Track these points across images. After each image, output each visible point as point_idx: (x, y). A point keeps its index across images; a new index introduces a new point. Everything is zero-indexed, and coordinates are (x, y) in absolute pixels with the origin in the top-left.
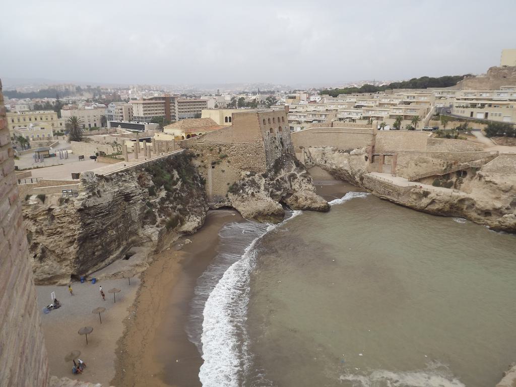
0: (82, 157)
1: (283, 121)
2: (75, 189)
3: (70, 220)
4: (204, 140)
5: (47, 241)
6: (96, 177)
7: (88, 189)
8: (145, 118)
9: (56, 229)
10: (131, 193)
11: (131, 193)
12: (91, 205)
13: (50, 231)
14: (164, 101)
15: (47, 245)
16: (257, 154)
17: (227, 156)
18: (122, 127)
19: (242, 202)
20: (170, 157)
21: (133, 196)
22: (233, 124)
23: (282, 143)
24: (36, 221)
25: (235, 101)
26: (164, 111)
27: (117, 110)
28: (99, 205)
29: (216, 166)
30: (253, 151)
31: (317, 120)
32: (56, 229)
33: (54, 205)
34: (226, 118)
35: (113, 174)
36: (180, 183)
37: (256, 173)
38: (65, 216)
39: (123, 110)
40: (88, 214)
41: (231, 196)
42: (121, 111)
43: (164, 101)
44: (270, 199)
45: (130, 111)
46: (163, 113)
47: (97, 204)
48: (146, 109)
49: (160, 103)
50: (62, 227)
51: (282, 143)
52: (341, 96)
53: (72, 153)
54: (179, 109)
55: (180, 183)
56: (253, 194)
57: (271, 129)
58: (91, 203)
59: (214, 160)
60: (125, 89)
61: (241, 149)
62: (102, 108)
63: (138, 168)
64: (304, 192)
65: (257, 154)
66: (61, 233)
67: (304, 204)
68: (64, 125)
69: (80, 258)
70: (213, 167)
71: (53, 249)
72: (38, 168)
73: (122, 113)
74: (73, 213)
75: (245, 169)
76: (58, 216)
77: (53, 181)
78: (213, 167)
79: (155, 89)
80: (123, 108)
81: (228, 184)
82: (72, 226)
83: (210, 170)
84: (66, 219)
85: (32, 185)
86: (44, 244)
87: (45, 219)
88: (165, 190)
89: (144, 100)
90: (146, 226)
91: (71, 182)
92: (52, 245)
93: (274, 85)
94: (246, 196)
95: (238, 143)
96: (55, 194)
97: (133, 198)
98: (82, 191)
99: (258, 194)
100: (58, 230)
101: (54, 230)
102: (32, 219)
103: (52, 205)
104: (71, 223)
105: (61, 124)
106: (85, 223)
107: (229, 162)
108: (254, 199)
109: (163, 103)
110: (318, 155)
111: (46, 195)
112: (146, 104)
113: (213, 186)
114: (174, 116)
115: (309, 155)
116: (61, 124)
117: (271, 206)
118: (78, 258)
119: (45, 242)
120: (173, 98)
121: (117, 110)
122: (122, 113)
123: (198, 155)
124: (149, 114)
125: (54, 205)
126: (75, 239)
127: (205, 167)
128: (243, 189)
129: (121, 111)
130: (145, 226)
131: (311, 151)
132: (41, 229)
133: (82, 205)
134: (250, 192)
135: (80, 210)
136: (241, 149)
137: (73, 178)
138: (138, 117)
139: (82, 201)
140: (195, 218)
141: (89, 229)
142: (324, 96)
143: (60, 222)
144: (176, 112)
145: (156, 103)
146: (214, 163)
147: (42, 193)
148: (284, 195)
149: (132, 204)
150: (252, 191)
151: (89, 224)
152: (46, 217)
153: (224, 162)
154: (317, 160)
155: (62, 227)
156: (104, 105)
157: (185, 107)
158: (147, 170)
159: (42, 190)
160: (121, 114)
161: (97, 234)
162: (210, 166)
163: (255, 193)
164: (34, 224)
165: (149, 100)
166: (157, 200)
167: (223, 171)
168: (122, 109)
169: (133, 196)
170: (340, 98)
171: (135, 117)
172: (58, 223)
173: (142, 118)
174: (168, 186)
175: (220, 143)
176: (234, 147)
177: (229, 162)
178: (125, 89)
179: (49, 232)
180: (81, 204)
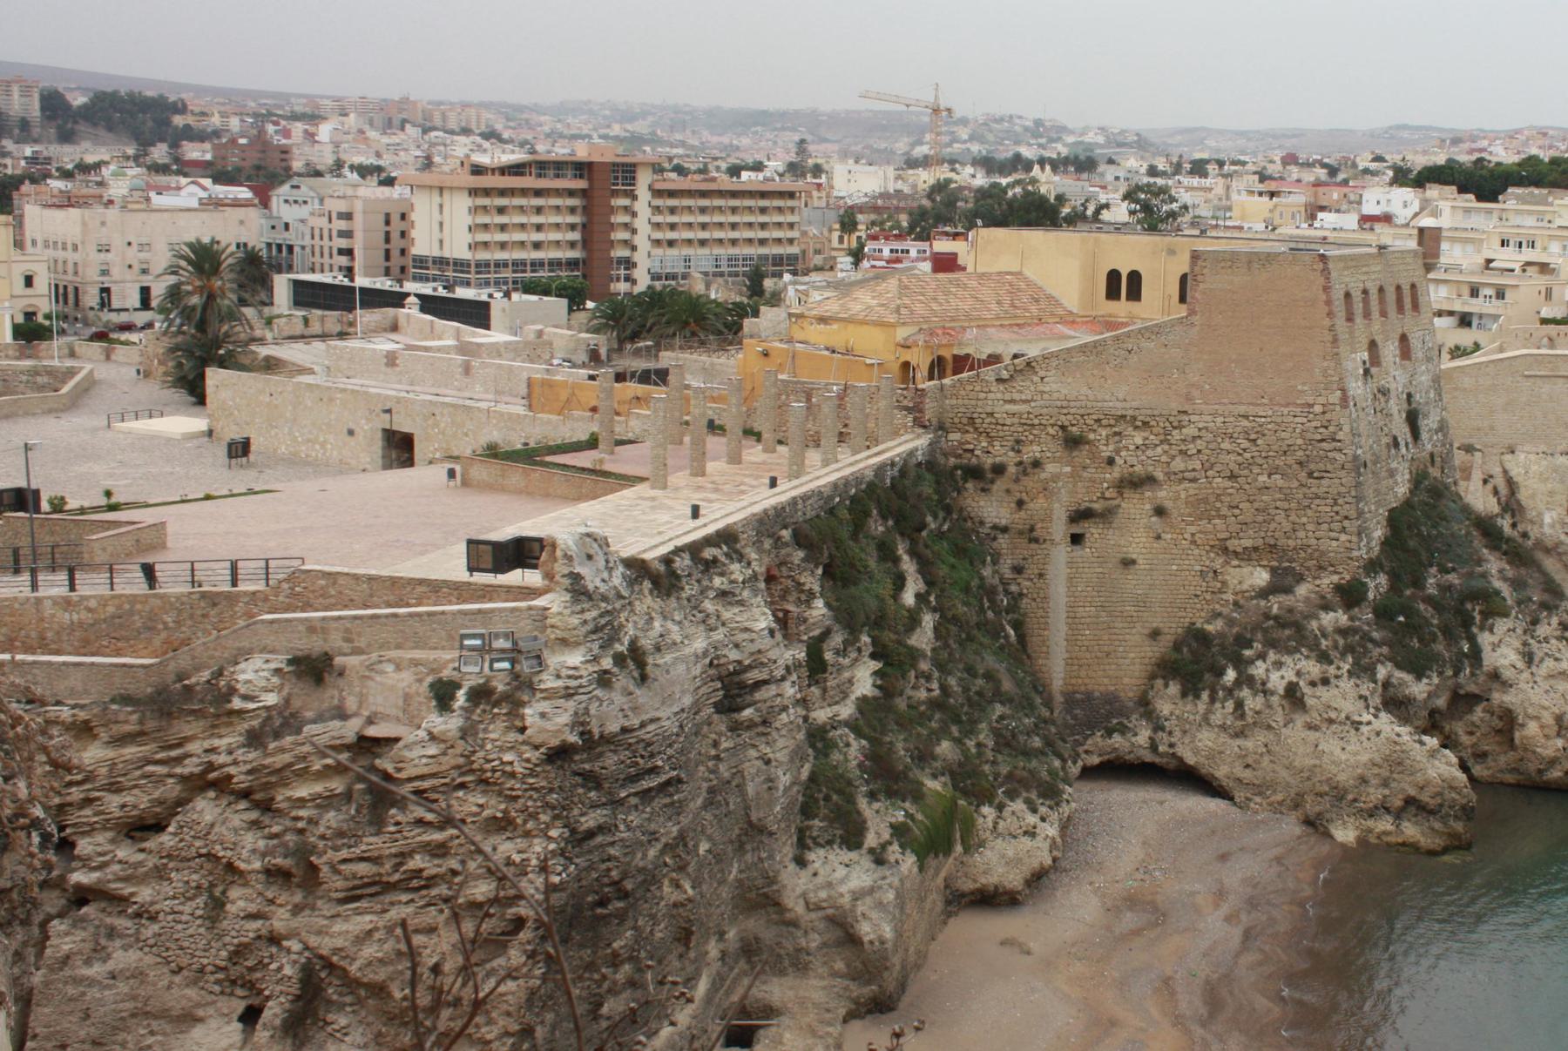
0: (400, 448)
1: (1416, 306)
2: (524, 628)
3: (496, 807)
4: (1025, 388)
5: (339, 927)
6: (621, 568)
7: (594, 632)
8: (482, 266)
9: (403, 856)
10: (750, 667)
11: (750, 667)
12: (613, 727)
13: (363, 868)
14: (581, 184)
15: (336, 951)
16: (1310, 475)
17: (1150, 480)
18: (423, 310)
19: (1237, 735)
20: (880, 469)
21: (759, 684)
22: (1192, 312)
23: (1412, 419)
24: (266, 807)
25: (951, 203)
26: (575, 236)
27: (322, 222)
28: (643, 725)
29: (1092, 530)
30: (1290, 460)
31: (1451, 313)
32: (403, 856)
33: (386, 717)
34: (1114, 276)
35: (678, 551)
36: (928, 620)
37: (1300, 579)
38: (462, 786)
39: (358, 224)
40: (592, 780)
41: (1168, 701)
42: (342, 225)
43: (581, 184)
44: (1386, 723)
45: (396, 226)
46: (572, 245)
47: (636, 722)
48: (486, 219)
49: (558, 193)
50: (439, 851)
51: (1412, 419)
52: (1518, 198)
53: (210, 433)
54: (657, 226)
55: (928, 620)
56: (1292, 692)
57: (1373, 345)
58: (610, 712)
59: (1086, 499)
60: (295, 117)
61: (1226, 445)
62: (237, 204)
63: (767, 524)
64: (1545, 685)
65: (1310, 475)
66: (431, 882)
67: (1549, 752)
68: (42, 284)
69: (540, 1032)
70: (1076, 539)
71: (381, 975)
72: (251, 492)
73: (347, 234)
74: (518, 769)
75: (1248, 556)
76: (426, 784)
77: (371, 579)
78: (1076, 539)
79: (453, 124)
80: (358, 208)
81: (1155, 634)
82: (505, 848)
83: (1060, 555)
84: (470, 803)
85: (231, 598)
86: (313, 941)
87: (326, 802)
88: (873, 656)
89: (478, 170)
90: (816, 856)
91: (459, 591)
92: (370, 951)
93: (1063, 129)
94: (1253, 702)
95: (1214, 414)
96: (394, 654)
97: (758, 696)
98: (564, 643)
99: (1321, 690)
100: (417, 862)
101: (388, 866)
102: (245, 794)
103: (370, 721)
104: (501, 825)
105: (29, 281)
106: (573, 831)
107: (1160, 511)
108: (1300, 720)
109: (571, 193)
110: (1551, 493)
111: (338, 660)
112: (487, 192)
113: (1071, 640)
114: (629, 264)
115: (1503, 491)
116: (29, 281)
117: (1396, 762)
118: (528, 1032)
119: (319, 933)
120: (627, 172)
121: (322, 222)
122: (347, 234)
123: (999, 470)
124: (503, 246)
125: (386, 717)
126: (519, 923)
127: (1031, 536)
128: (1240, 663)
129: (342, 225)
130: (811, 856)
131: (1515, 472)
132: (303, 853)
133: (573, 726)
134: (1277, 681)
135: (559, 755)
136: (1226, 445)
137: (471, 569)
138: (441, 262)
139: (571, 704)
140: (1032, 819)
141: (590, 868)
142: (1433, 191)
143: (430, 817)
144: (641, 241)
145: (538, 193)
146: (1081, 515)
147: (314, 645)
148: (1441, 702)
149: (751, 725)
150: (1290, 676)
151: (591, 834)
152: (337, 785)
153: (1136, 507)
154: (1547, 519)
155: (439, 851)
156: (244, 193)
157: (718, 218)
158: (800, 540)
159: (311, 628)
160: (343, 243)
161: (625, 895)
162: (1059, 529)
163: (1307, 690)
164: (255, 825)
165: (504, 170)
166: (846, 711)
167: (1128, 563)
168: (348, 216)
169: (759, 684)
170: (1511, 204)
171: (420, 262)
172: (420, 822)
173: (461, 265)
174: (888, 637)
175: (1118, 408)
176: (1190, 431)
177: (1160, 511)
178: (295, 117)
179: (354, 876)
180: (564, 719)
